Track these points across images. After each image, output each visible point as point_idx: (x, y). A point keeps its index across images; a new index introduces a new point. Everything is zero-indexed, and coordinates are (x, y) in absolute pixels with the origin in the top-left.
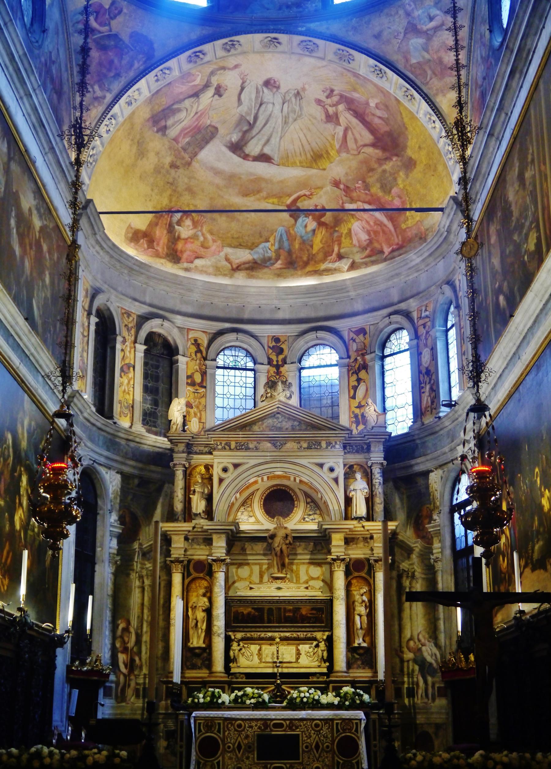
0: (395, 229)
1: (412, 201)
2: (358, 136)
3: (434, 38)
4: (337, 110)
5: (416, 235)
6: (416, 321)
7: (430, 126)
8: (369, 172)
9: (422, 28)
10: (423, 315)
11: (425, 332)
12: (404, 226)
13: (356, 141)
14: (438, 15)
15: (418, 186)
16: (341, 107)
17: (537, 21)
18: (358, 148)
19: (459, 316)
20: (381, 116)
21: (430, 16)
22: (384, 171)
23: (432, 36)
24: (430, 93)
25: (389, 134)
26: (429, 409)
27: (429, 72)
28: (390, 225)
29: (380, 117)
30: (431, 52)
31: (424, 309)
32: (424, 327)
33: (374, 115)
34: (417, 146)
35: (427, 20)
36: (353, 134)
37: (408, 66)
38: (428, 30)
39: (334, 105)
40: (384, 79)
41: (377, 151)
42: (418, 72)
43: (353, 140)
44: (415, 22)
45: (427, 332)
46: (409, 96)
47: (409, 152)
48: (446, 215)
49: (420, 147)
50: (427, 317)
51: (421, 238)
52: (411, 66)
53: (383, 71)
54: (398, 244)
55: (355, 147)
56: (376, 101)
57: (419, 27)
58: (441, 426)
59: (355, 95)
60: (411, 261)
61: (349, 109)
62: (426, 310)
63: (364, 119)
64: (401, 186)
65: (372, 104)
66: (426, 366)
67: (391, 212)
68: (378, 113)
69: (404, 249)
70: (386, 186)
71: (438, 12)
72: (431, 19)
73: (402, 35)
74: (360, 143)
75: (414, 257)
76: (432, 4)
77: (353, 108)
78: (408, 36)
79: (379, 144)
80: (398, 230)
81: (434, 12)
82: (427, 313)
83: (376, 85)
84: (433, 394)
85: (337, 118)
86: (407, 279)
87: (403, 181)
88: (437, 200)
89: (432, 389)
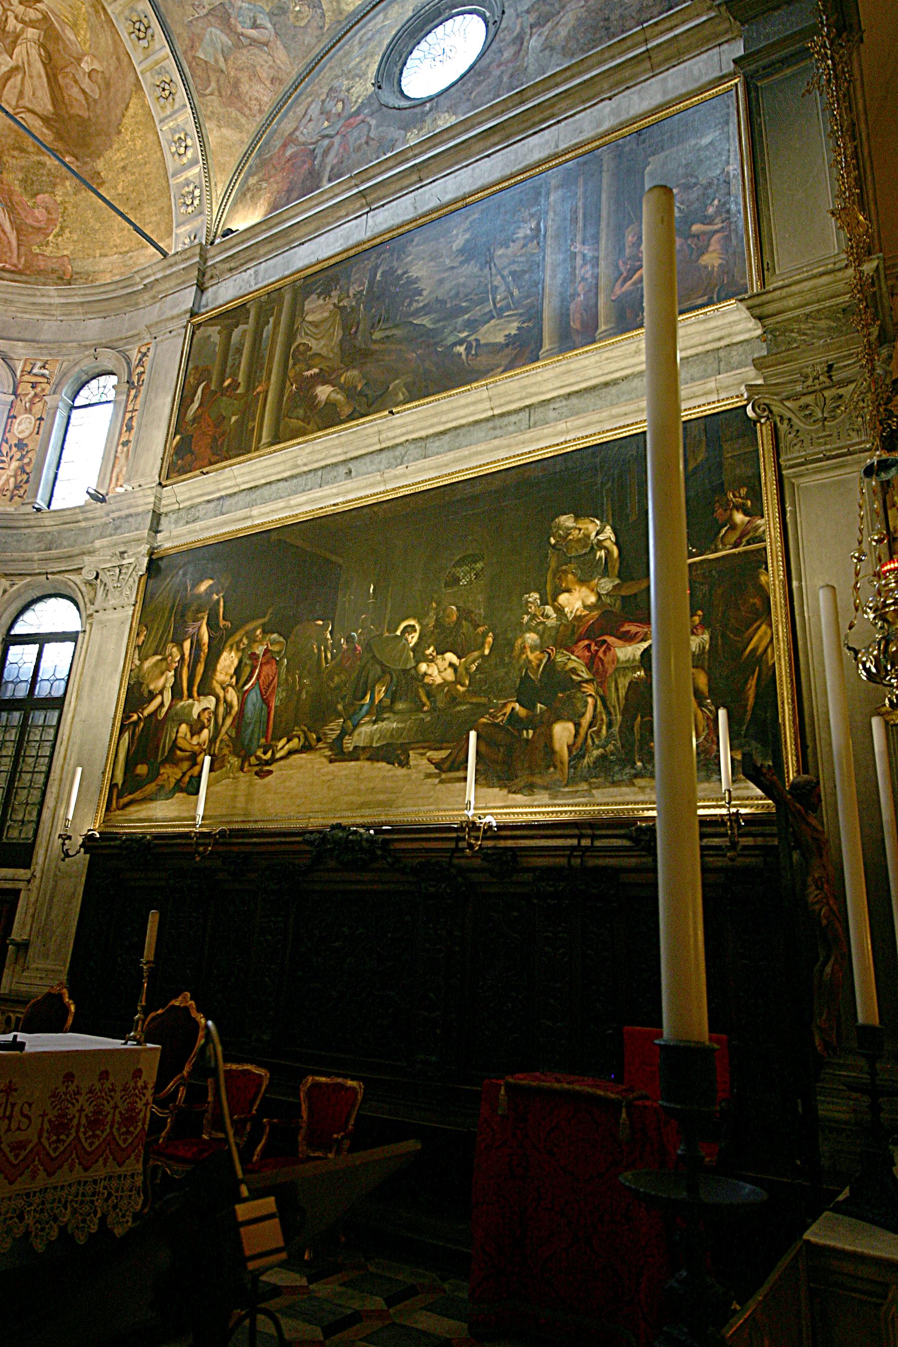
0: (19, 245)
1: (67, 227)
2: (28, 91)
3: (245, 51)
4: (22, 31)
5: (53, 271)
6: (18, 374)
7: (173, 149)
8: (14, 149)
9: (236, 26)
10: (35, 371)
11: (33, 393)
12: (36, 249)
13: (21, 95)
14: (265, 28)
15: (89, 213)
16: (31, 33)
17: (606, 86)
18: (17, 106)
19: (128, 396)
20: (87, 90)
21: (255, 21)
22: (42, 164)
23: (244, 47)
24: (202, 111)
25: (84, 123)
26: (8, 494)
27: (213, 85)
28: (13, 237)
29: (83, 91)
30: (230, 62)
31: (39, 364)
32: (33, 387)
33: (76, 81)
34: (122, 164)
35: (249, 23)
36: (22, 84)
37: (189, 54)
38: (242, 34)
39: (23, 21)
40: (144, 43)
41: (45, 131)
42: (199, 72)
43: (17, 91)
44: (230, 11)
45: (36, 395)
46: (167, 92)
47: (100, 165)
48: (165, 263)
49: (124, 168)
50: (43, 376)
51: (61, 278)
52: (194, 57)
53: (150, 32)
54: (16, 266)
55: (14, 103)
56: (96, 66)
57: (232, 21)
58: (32, 523)
59: (70, 34)
60: (43, 296)
61: (42, 46)
62: (44, 367)
63: (55, 76)
64: (59, 199)
65: (85, 66)
66: (21, 436)
67: (104, 205)
68: (86, 83)
69: (24, 278)
70: (32, 184)
71: (269, 26)
72: (255, 26)
73: (205, 11)
74: (25, 102)
75: (52, 295)
76: (267, 10)
77: (50, 47)
78: (210, 18)
79: (57, 125)
80: (22, 249)
81: (263, 20)
82: (46, 372)
83: (117, 41)
84: (25, 477)
85: (14, 44)
86: (19, 315)
87: (66, 194)
88: (116, 246)
89: (22, 469)
